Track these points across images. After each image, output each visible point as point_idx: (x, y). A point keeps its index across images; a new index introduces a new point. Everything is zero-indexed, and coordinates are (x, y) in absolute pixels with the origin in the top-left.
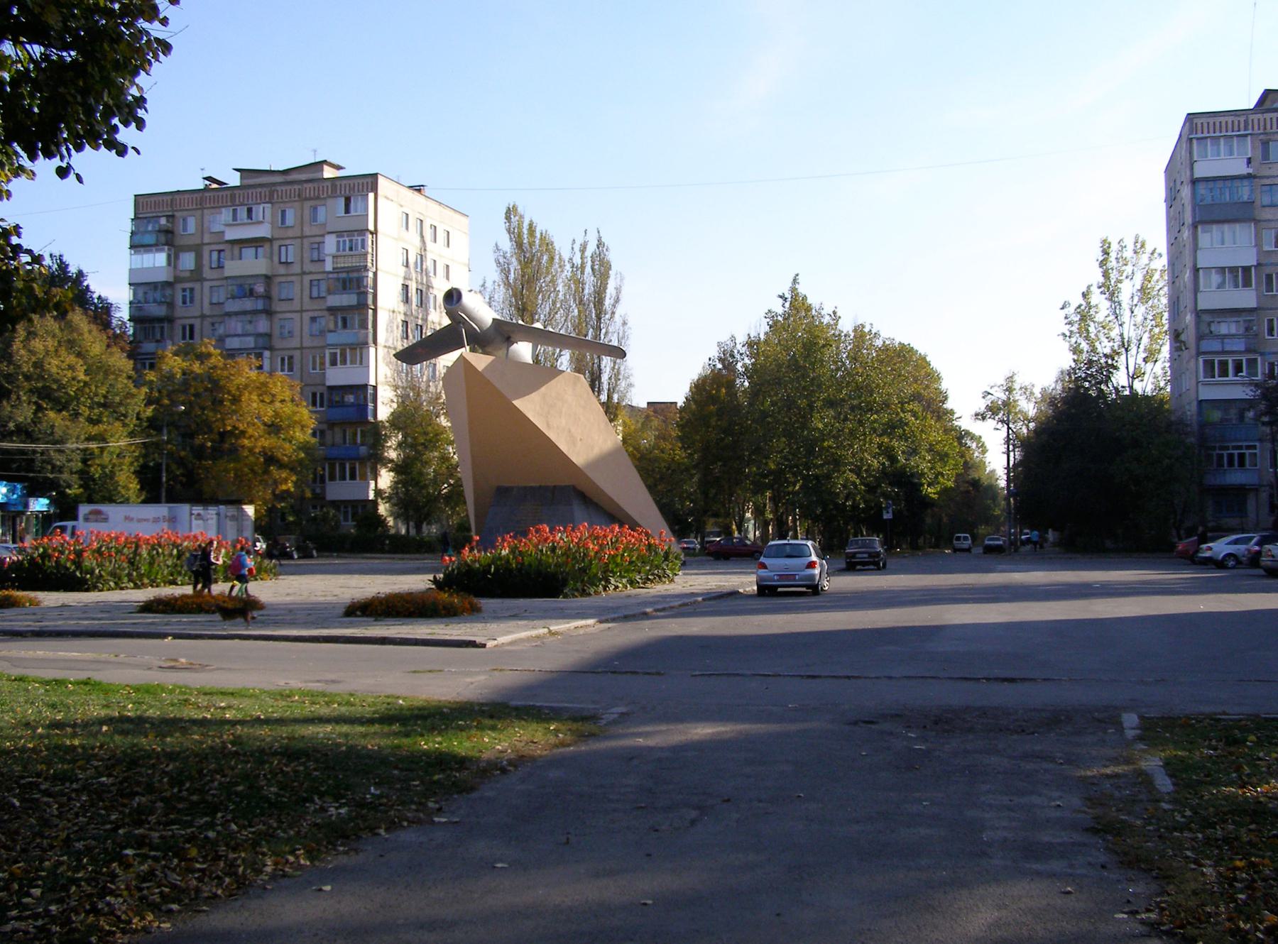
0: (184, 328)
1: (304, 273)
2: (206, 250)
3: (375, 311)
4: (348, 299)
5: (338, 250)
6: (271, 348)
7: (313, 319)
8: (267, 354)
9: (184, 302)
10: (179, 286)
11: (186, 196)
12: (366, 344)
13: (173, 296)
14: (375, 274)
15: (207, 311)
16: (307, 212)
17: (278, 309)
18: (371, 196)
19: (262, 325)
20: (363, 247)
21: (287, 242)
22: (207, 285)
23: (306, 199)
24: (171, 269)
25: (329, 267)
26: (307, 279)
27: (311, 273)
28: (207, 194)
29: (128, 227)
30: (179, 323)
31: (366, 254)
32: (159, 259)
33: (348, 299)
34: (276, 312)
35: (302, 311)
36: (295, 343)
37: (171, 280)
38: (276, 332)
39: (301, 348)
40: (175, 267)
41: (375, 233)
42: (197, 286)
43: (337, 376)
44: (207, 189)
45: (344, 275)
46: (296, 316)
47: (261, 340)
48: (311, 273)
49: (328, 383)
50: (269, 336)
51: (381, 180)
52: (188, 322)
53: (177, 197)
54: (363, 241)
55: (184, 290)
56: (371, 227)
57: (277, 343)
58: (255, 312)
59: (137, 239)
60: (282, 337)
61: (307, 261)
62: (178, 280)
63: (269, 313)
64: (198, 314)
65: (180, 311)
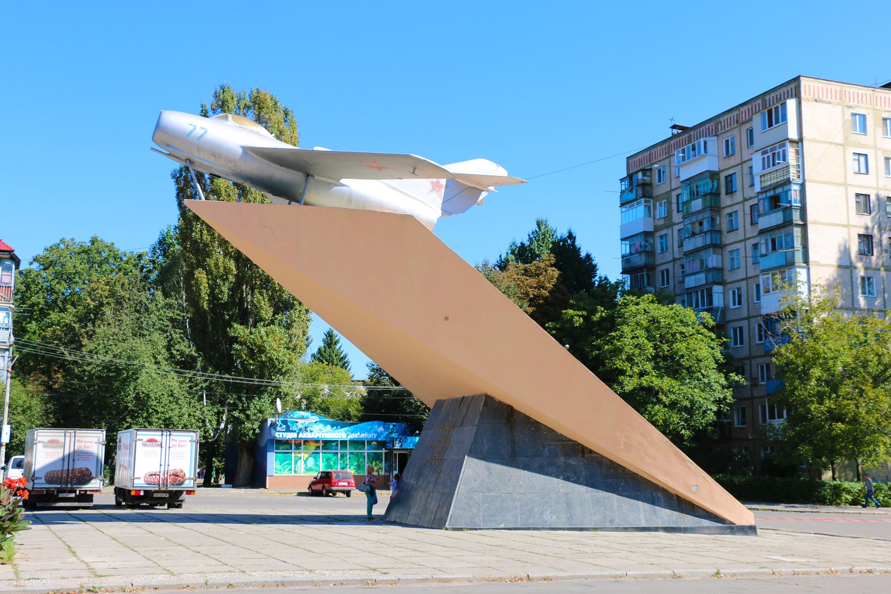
0: (663, 272)
1: (745, 200)
2: (674, 194)
3: (804, 227)
4: (776, 218)
5: (764, 168)
6: (722, 283)
7: (755, 246)
8: (717, 289)
9: (662, 250)
10: (658, 234)
11: (659, 148)
12: (791, 264)
13: (653, 245)
14: (803, 186)
15: (677, 256)
16: (744, 136)
17: (727, 242)
18: (791, 104)
19: (713, 260)
20: (784, 160)
21: (731, 172)
22: (676, 228)
23: (743, 123)
24: (652, 219)
25: (757, 188)
26: (748, 204)
27: (751, 198)
28: (672, 142)
29: (618, 187)
30: (659, 268)
31: (788, 167)
32: (639, 211)
33: (776, 218)
34: (726, 245)
35: (745, 239)
36: (741, 274)
37: (651, 229)
38: (727, 265)
39: (747, 279)
40: (654, 218)
41: (801, 140)
42: (669, 231)
43: (769, 305)
44: (674, 136)
45: (771, 193)
46: (740, 246)
47: (710, 275)
48: (751, 198)
49: (764, 312)
50: (721, 270)
51: (804, 82)
52: (664, 267)
53: (653, 151)
54: (784, 151)
55: (661, 237)
56: (793, 134)
57: (728, 277)
58: (705, 248)
59: (626, 199)
60: (732, 269)
61: (747, 185)
62: (657, 228)
63: (718, 247)
64: (670, 258)
65: (658, 260)
